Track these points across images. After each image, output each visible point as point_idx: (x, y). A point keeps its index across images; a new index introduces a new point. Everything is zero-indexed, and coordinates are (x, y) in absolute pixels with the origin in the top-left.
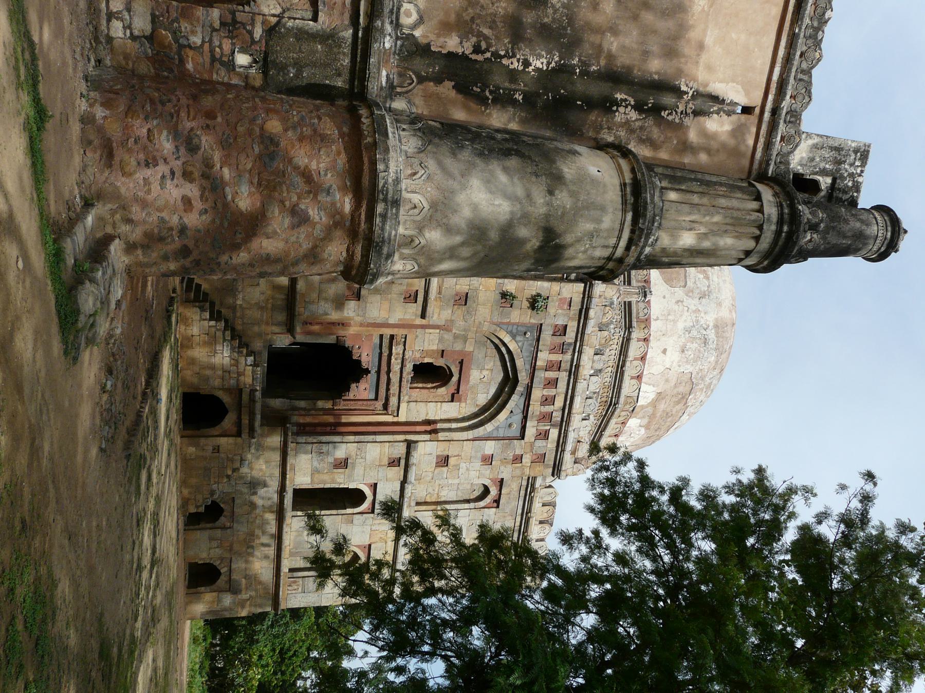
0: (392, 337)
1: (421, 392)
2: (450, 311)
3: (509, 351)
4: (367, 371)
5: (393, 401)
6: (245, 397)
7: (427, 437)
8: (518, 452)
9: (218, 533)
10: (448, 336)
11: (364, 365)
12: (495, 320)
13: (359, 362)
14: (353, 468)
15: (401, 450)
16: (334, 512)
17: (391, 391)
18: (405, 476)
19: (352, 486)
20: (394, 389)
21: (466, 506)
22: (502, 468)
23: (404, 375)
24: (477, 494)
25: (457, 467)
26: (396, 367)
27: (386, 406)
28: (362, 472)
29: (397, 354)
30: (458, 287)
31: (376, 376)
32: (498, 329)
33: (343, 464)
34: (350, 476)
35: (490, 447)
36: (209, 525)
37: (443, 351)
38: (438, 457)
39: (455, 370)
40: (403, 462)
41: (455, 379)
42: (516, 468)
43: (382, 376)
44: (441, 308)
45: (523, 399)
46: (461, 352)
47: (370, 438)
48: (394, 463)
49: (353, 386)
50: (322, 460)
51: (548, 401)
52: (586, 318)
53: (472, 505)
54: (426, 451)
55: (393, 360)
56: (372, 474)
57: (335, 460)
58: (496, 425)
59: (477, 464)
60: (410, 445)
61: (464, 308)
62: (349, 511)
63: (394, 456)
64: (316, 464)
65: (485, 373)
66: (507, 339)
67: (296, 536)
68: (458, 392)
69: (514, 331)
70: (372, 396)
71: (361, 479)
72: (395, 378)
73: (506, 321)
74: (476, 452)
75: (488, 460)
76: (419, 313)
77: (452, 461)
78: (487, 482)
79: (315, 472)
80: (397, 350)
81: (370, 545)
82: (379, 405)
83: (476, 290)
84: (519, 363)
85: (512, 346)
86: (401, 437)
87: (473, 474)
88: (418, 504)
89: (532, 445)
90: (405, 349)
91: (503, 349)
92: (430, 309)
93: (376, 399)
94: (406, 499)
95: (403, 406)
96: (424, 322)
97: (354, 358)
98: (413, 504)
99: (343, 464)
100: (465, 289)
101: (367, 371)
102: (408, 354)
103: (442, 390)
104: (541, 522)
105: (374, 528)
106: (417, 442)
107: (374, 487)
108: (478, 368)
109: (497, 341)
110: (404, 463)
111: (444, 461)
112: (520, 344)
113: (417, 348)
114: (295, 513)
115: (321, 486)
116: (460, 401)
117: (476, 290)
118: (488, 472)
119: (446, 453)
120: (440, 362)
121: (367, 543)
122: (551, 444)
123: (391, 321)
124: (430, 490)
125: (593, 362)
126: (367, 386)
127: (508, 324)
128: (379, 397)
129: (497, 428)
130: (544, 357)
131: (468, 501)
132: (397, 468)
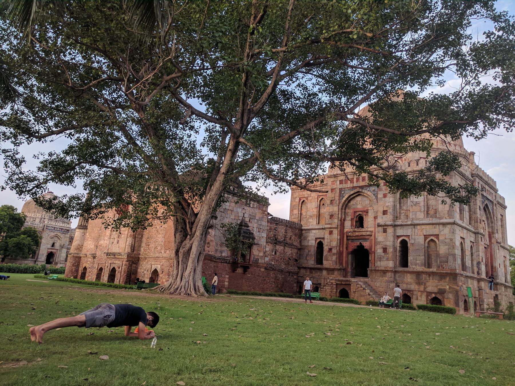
5: (368, 233)
6: (339, 283)
14: (387, 246)
28: (388, 242)
33: (385, 250)
40: (385, 227)
41: (361, 213)
59: (387, 199)
64: (385, 259)
79: (388, 259)
95: (369, 230)
104: (417, 165)
105: (416, 235)
132: (387, 230)
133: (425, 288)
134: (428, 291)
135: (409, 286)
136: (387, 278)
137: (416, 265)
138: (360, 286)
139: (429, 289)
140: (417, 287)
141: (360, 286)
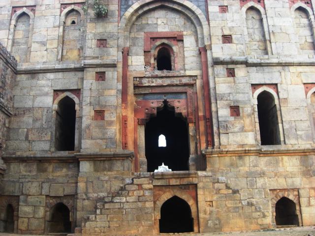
0: (136, 87)
1: (177, 64)
2: (111, 49)
3: (142, 7)
4: (165, 102)
7: (209, 52)
9: (304, 201)
10: (134, 50)
11: (161, 104)
12: (116, 19)
13: (158, 108)
14: (237, 101)
15: (221, 70)
16: (279, 113)
17: (178, 83)
18: (242, 63)
19: (255, 102)
20: (176, 81)
21: (265, 20)
23: (164, 75)
24: (256, 16)
25: (231, 29)
26: (159, 82)
27: (192, 85)
28: (241, 95)
29: (149, 82)
30: (93, 46)
31: (169, 96)
32: (124, 17)
33: (235, 110)
34: (245, 103)
36: (298, 208)
37: (145, 52)
38: (224, 42)
39: (158, 43)
40: (230, 66)
41: (166, 41)
43: (168, 91)
44: (108, 55)
46: (145, 40)
47: (212, 91)
48: (231, 73)
49: (177, 111)
50: (233, 125)
53: (264, 16)
54: (219, 51)
55: (154, 84)
56: (242, 87)
57: (232, 115)
59: (227, 15)
60: (217, 62)
61: (108, 41)
62: (277, 102)
63: (226, 73)
65: (159, 22)
66: (131, 10)
67: (302, 139)
68: (176, 37)
69: (125, 6)
70: (183, 96)
71: (247, 95)
72: (167, 82)
73: (117, 13)
74: (218, 17)
76: (112, 69)
77: (227, 33)
78: (244, 9)
79: (243, 130)
80: (146, 82)
81: (304, 84)
82: (190, 91)
83: (95, 35)
85: (136, 6)
86: (210, 70)
87: (236, 17)
88: (267, 53)
90: (144, 77)
91: (140, 12)
92: (108, 61)
93: (186, 93)
94: (262, 61)
95: (188, 73)
96: (120, 66)
97: (155, 112)
98: (266, 57)
99: (235, 110)
100: (94, 42)
101: (165, 102)
102: (148, 74)
103: (175, 48)
105: (289, 82)
106: (213, 59)
107: (254, 86)
108: (157, 28)
109: (134, 18)
110: (230, 67)
111: (227, 39)
113: (144, 69)
114: (282, 143)
115: (258, 125)
116: (182, 36)
117: (95, 35)
118: (233, 7)
119: (221, 38)
120: (155, 52)
121: (303, 86)
123: (120, 87)
124: (255, 47)
126: (176, 100)
127: (120, 10)
128: (185, 91)
129: (199, 6)
131: (261, 20)
132: (236, 71)
135: (290, 181)
136: (247, 169)
137: (297, 139)
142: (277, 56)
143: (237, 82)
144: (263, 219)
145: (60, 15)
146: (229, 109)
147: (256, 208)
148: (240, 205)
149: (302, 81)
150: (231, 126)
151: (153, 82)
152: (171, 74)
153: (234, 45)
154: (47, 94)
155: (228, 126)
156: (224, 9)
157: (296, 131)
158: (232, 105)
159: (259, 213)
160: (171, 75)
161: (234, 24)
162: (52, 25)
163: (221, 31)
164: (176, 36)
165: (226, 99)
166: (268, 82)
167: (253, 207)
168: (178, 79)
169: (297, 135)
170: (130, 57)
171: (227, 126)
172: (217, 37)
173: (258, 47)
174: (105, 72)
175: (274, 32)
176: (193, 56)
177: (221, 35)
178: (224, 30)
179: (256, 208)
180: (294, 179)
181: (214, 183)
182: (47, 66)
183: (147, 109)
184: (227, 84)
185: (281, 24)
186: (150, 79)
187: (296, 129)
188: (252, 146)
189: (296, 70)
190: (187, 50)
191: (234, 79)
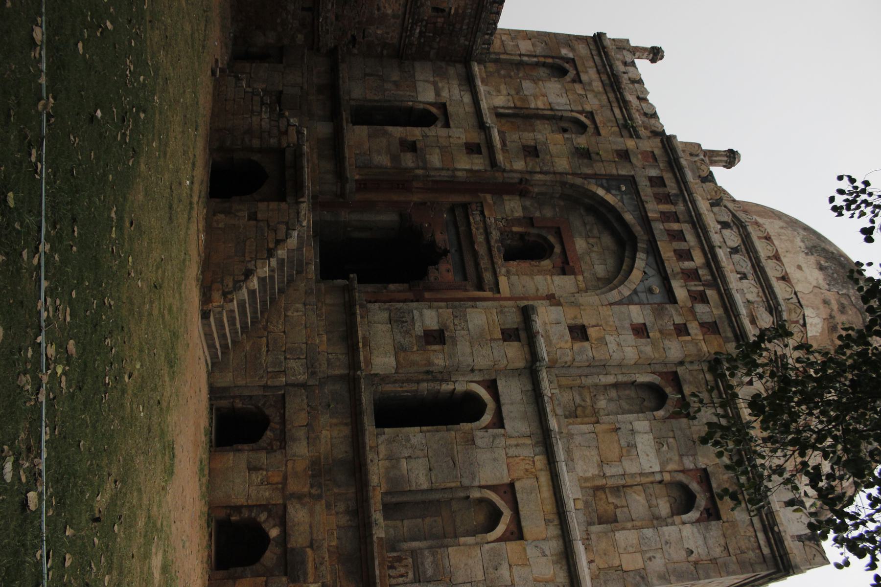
3: (611, 209)
4: (446, 252)
5: (488, 276)
8: (678, 320)
13: (433, 243)
20: (484, 263)
22: (666, 342)
26: (480, 239)
28: (468, 350)
33: (437, 337)
35: (637, 314)
39: (552, 239)
41: (557, 250)
42: (685, 342)
45: (651, 259)
48: (508, 335)
49: (431, 269)
50: (407, 332)
51: (684, 255)
52: (681, 168)
58: (633, 287)
64: (399, 337)
66: (601, 192)
68: (568, 264)
72: (482, 250)
75: (640, 331)
79: (399, 350)
84: (629, 217)
85: (609, 198)
89: (692, 310)
93: (465, 278)
103: (546, 263)
105: (512, 451)
112: (619, 197)
121: (506, 480)
122: (718, 312)
125: (715, 214)
130: (653, 209)
133: (299, 497)
134: (291, 510)
135: (301, 433)
137: (389, 458)
138: (281, 235)
139: (298, 514)
140: (301, 465)
141: (281, 235)
142: (565, 431)
143: (493, 345)
144: (220, 292)
145: (572, 111)
146: (436, 327)
147: (240, 281)
148: (248, 259)
149: (518, 479)
150: (404, 329)
151: (477, 229)
152: (499, 261)
153: (569, 345)
154: (438, 93)
155: (405, 324)
156: (640, 331)
157: (406, 458)
158: (446, 334)
159: (231, 285)
160: (494, 253)
161: (612, 346)
162: (550, 101)
163: (593, 322)
164: (571, 264)
165: (456, 322)
166: (505, 410)
167: (243, 278)
168: (489, 266)
169: (398, 460)
170: (518, 198)
171: (403, 322)
172: (579, 316)
173: (580, 406)
174: (481, 153)
175: (619, 433)
176: (537, 290)
177: (586, 323)
178: (598, 328)
179: (240, 281)
180: (305, 443)
181: (287, 224)
182: (483, 97)
183: (430, 225)
184: (487, 328)
185: (639, 446)
186: (482, 225)
187: (410, 457)
188: (369, 363)
189: (541, 470)
190: (546, 280)
191: (499, 339)
